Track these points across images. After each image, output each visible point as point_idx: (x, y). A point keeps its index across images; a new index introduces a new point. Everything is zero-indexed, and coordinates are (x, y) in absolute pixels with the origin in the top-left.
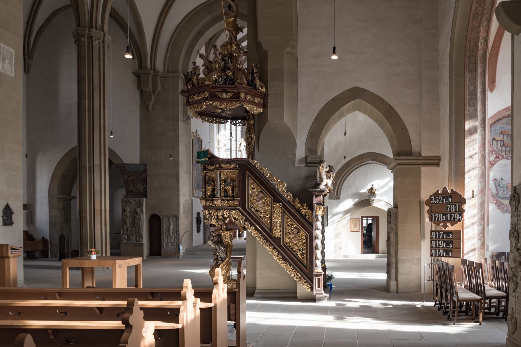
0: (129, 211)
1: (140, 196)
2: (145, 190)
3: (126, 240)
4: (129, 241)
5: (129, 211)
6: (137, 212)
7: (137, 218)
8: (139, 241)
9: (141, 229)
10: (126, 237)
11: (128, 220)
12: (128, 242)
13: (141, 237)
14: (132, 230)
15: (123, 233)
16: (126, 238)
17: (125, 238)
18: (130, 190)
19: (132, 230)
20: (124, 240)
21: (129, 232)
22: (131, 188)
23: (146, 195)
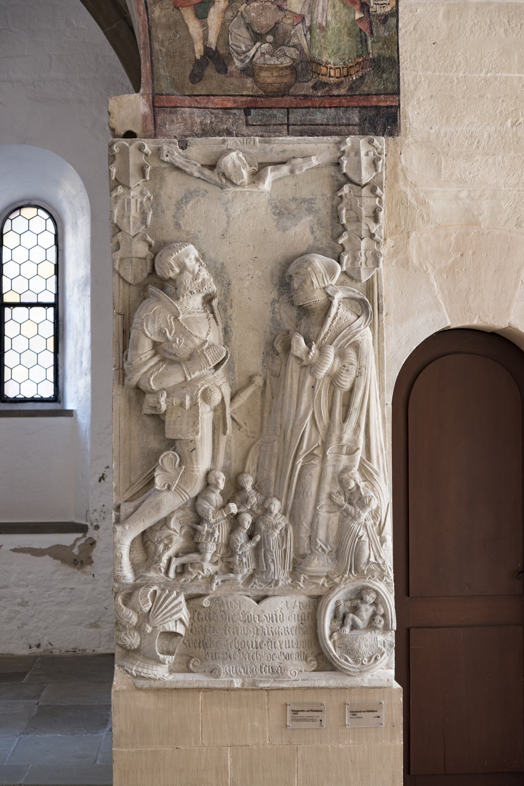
0: (213, 287)
1: (319, 117)
2: (373, 51)
3: (169, 659)
4: (224, 668)
5: (213, 287)
6: (319, 297)
7: (322, 373)
8: (349, 664)
9: (365, 515)
10: (184, 614)
11: (206, 396)
12: (213, 672)
13: (366, 611)
14: (247, 520)
15: (135, 568)
16: (181, 630)
17: (171, 626)
18: (199, 48)
19: (247, 520)
20: (157, 645)
21: (211, 548)
22: (205, 27)
23: (385, 102)
